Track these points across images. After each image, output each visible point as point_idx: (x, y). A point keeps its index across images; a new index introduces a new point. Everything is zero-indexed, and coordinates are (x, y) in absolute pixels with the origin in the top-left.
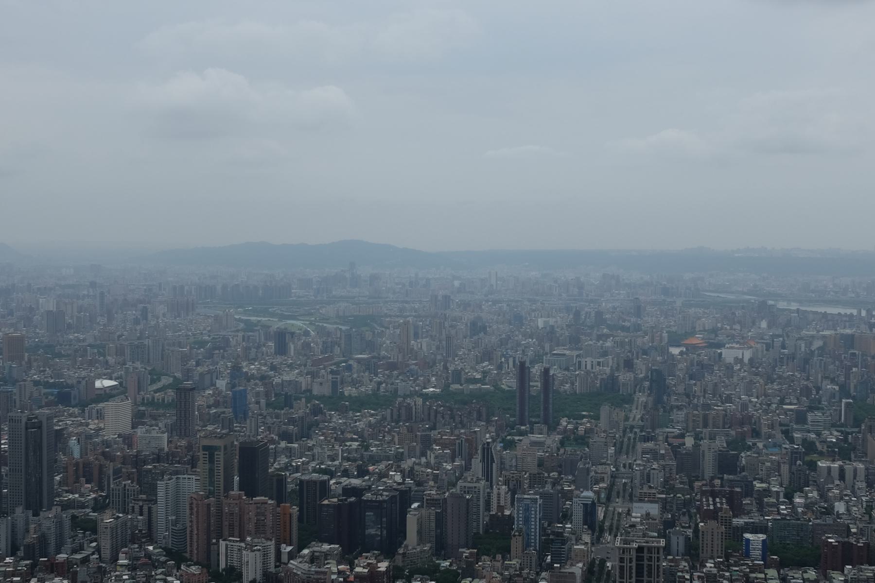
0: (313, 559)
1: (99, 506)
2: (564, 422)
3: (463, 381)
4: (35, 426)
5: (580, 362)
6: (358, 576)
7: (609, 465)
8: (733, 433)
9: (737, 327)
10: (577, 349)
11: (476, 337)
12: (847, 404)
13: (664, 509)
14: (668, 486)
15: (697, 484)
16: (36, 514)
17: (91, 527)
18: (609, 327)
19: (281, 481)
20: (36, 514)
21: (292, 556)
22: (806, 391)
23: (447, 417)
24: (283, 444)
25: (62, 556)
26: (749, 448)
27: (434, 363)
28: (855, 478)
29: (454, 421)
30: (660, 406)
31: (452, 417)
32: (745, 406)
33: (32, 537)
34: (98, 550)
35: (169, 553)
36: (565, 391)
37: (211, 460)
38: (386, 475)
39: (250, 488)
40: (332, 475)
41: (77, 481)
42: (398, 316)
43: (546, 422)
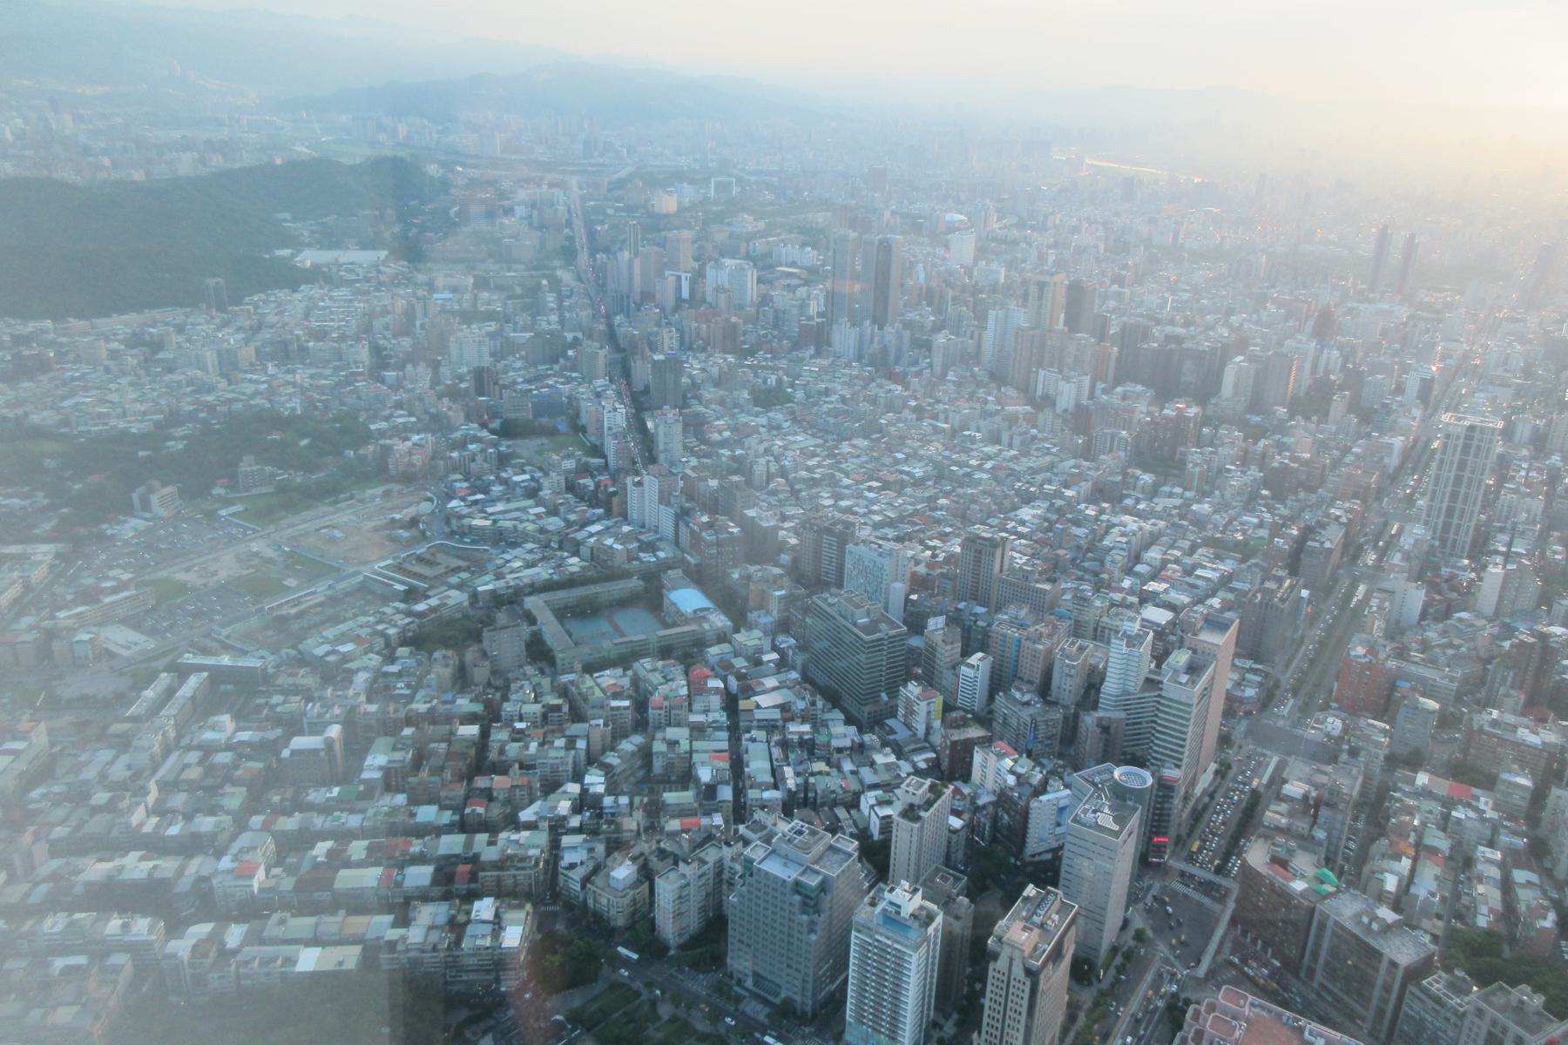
0: (1125, 397)
1: (936, 329)
4: (886, 247)
6: (1167, 418)
13: (1517, 396)
16: (881, 328)
17: (927, 346)
19: (1105, 323)
20: (881, 328)
21: (1105, 391)
24: (1115, 287)
25: (898, 369)
33: (876, 346)
34: (931, 365)
35: (992, 375)
37: (1040, 297)
38: (1213, 328)
39: (1073, 323)
40: (1158, 322)
41: (919, 304)
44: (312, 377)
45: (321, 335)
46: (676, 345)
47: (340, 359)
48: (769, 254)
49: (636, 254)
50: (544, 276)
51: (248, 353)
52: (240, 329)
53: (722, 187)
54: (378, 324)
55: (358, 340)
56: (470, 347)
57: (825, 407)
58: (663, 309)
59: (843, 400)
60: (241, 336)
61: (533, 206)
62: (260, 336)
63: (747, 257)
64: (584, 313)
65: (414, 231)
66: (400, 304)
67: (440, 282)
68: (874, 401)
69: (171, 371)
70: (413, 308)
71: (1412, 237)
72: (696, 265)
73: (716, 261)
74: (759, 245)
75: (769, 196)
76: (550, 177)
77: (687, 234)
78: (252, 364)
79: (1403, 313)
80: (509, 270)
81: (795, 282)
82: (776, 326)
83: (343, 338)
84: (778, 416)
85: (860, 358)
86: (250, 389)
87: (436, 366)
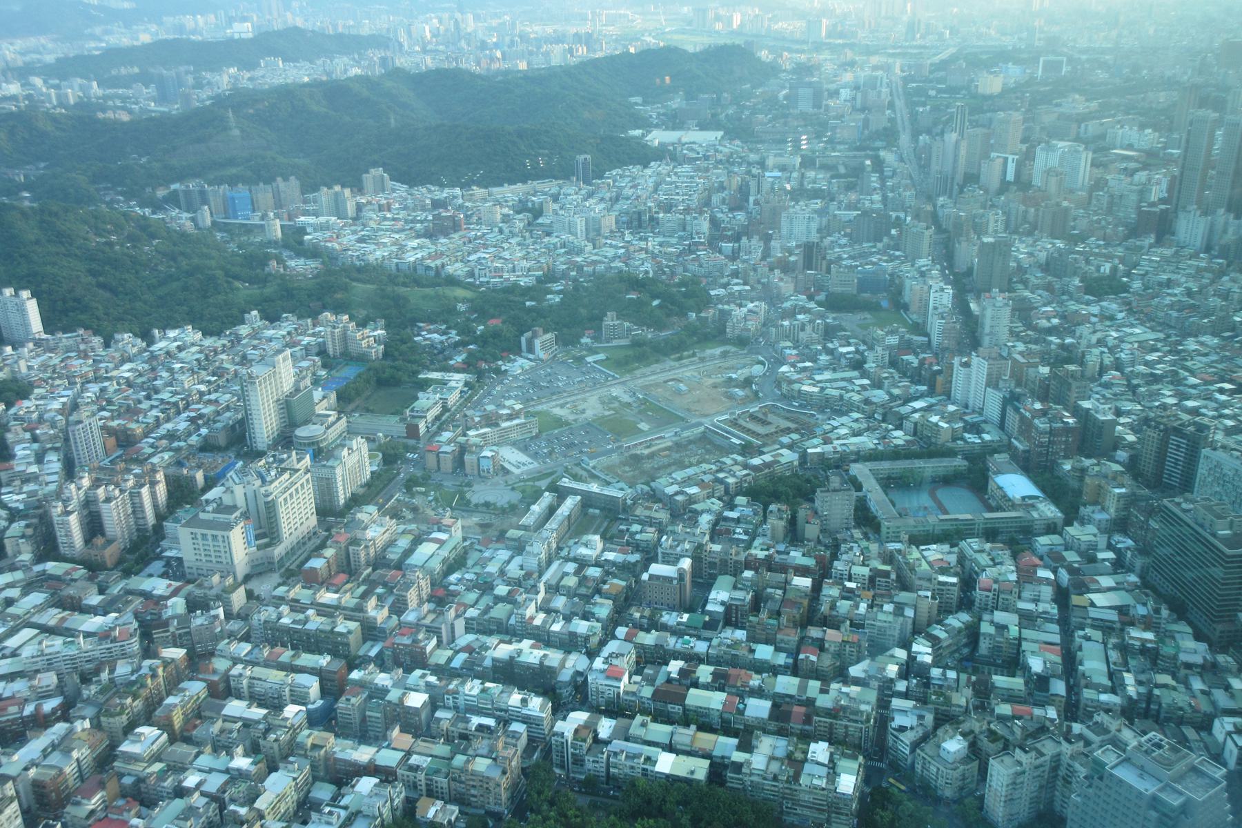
44: (661, 244)
45: (668, 207)
46: (1000, 227)
47: (684, 230)
48: (1103, 136)
49: (962, 134)
50: (867, 157)
51: (609, 222)
52: (602, 199)
53: (1049, 66)
54: (716, 198)
55: (701, 213)
56: (800, 225)
57: (1168, 300)
58: (986, 191)
59: (1189, 293)
60: (602, 206)
61: (857, 88)
62: (617, 207)
63: (1078, 139)
64: (908, 193)
65: (747, 113)
66: (737, 180)
67: (770, 161)
68: (1226, 296)
69: (549, 234)
70: (747, 185)
72: (1024, 147)
73: (1047, 143)
74: (1092, 128)
75: (1102, 75)
76: (875, 60)
77: (1017, 116)
78: (612, 232)
80: (834, 150)
81: (1133, 165)
82: (1109, 211)
83: (687, 211)
84: (1111, 305)
85: (1208, 249)
86: (610, 252)
87: (767, 239)
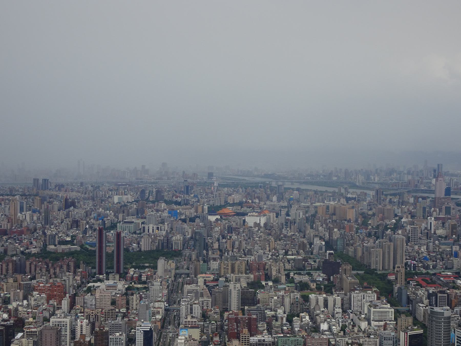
2: (131, 271)
3: (57, 243)
5: (144, 228)
7: (162, 302)
8: (252, 276)
9: (257, 201)
10: (142, 218)
11: (67, 210)
12: (330, 254)
14: (205, 316)
15: (226, 315)
18: (167, 202)
22: (303, 246)
23: (44, 270)
26: (263, 287)
27: (35, 230)
28: (334, 305)
29: (49, 273)
30: (201, 258)
31: (48, 270)
32: (260, 257)
36: (133, 249)
42: (8, 195)
43: (118, 272)
71: (118, 235)
79: (121, 286)
